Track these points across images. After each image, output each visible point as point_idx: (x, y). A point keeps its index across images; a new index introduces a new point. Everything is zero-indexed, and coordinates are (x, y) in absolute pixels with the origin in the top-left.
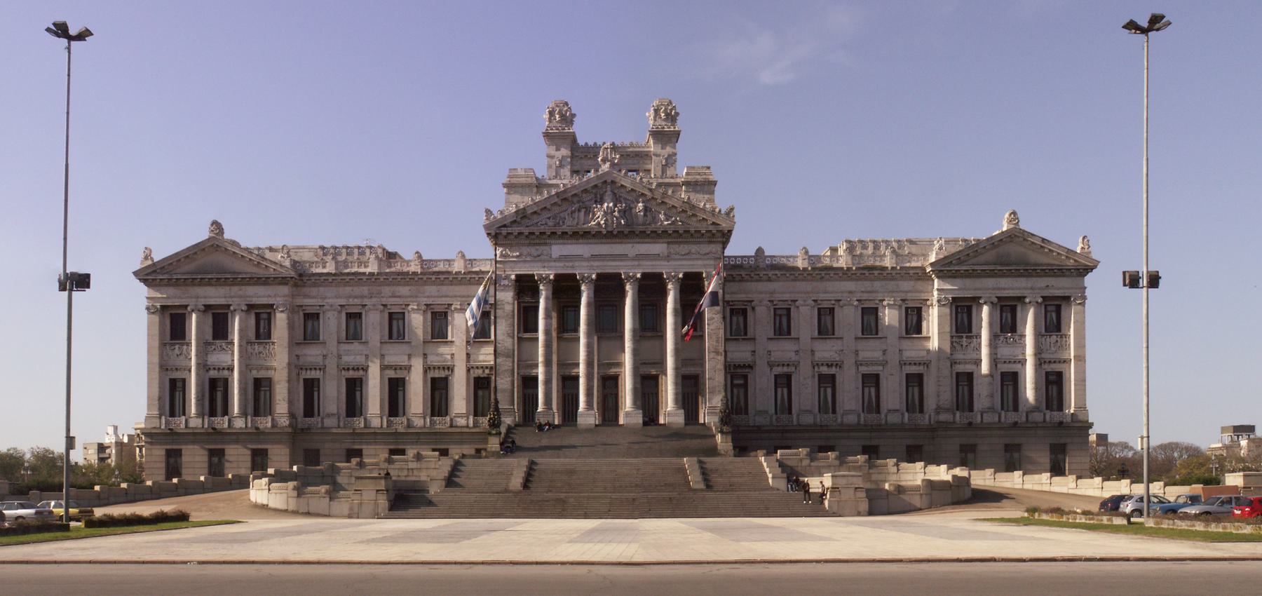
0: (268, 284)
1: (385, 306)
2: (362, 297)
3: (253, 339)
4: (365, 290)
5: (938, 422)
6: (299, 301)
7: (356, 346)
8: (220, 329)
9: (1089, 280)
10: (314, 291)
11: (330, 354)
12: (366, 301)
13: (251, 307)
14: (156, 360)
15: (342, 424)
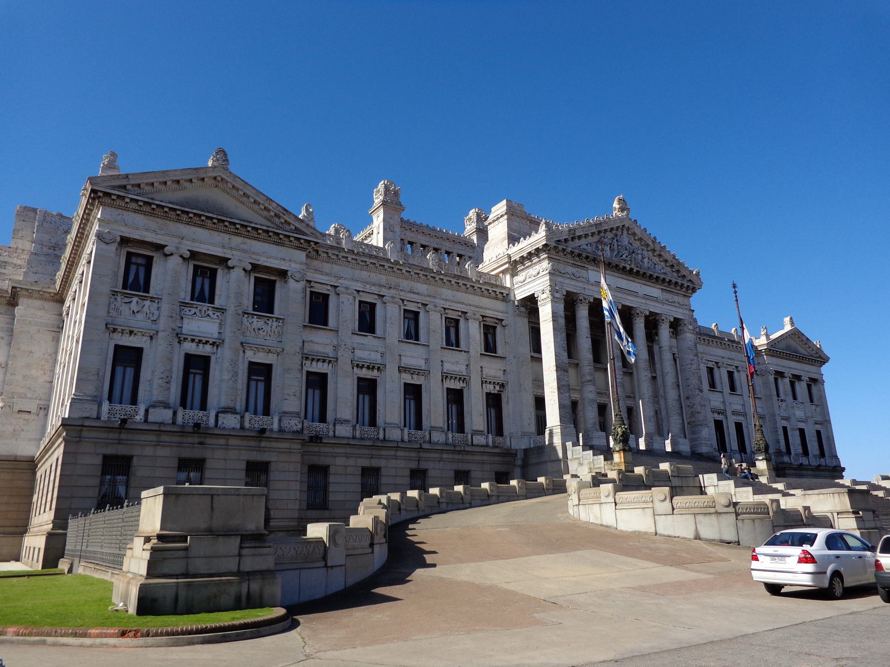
0: (282, 244)
1: (403, 300)
2: (380, 286)
3: (251, 310)
4: (383, 279)
5: (783, 463)
6: (311, 276)
7: (368, 340)
8: (204, 290)
9: (824, 369)
10: (327, 267)
11: (342, 347)
12: (384, 291)
13: (255, 267)
14: (102, 312)
15: (358, 435)
